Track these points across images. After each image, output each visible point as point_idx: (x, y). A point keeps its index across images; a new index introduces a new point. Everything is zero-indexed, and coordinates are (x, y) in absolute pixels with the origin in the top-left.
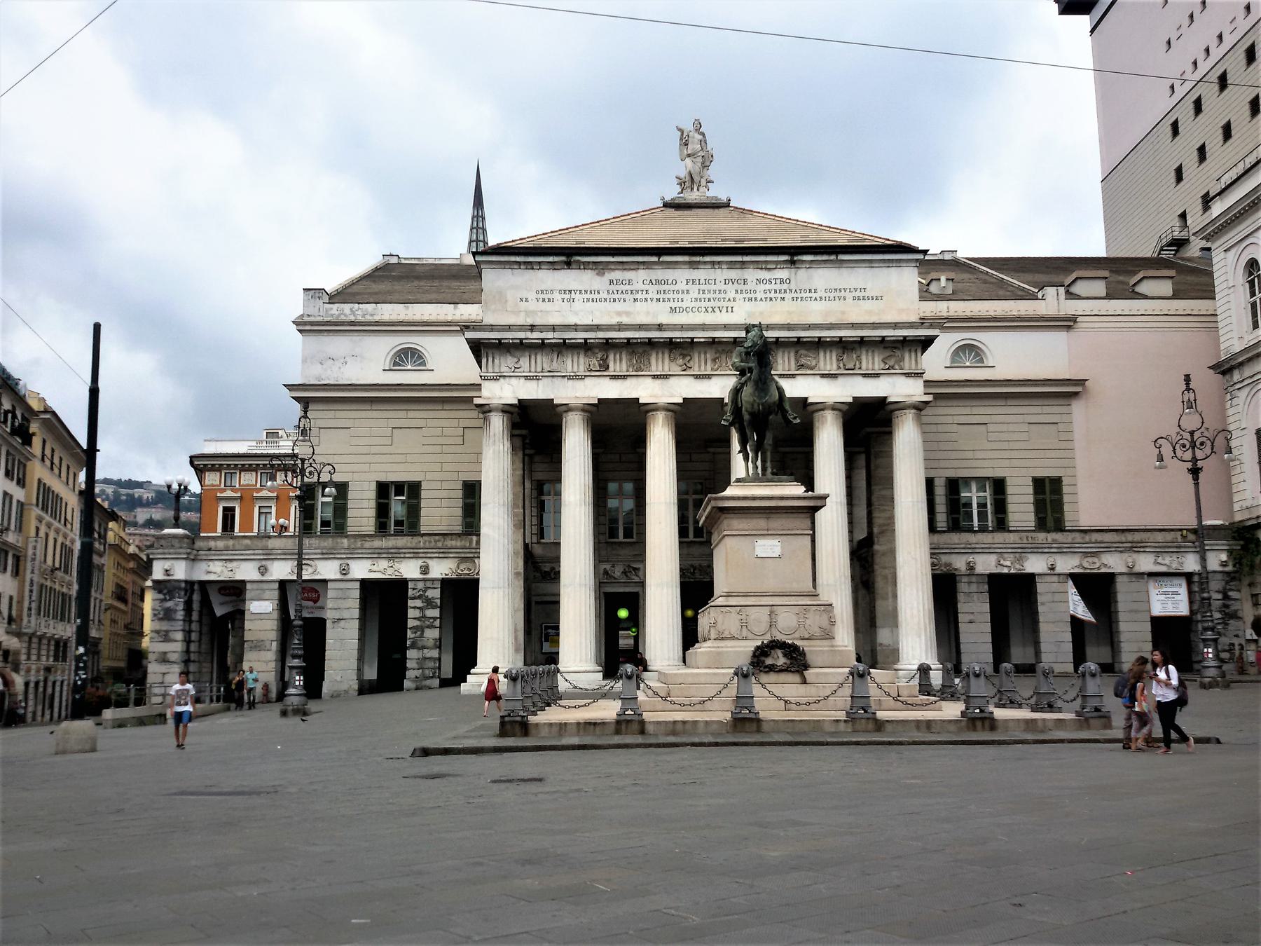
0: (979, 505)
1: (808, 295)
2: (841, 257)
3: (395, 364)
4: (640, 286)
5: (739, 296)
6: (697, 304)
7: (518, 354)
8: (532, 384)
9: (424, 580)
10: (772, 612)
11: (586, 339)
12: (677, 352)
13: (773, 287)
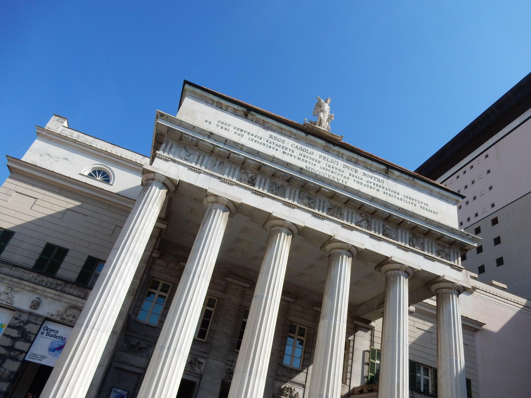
0: (424, 385)
1: (393, 194)
2: (415, 180)
3: (90, 175)
4: (289, 147)
5: (351, 177)
7: (190, 151)
8: (194, 175)
9: (30, 314)
13: (372, 180)
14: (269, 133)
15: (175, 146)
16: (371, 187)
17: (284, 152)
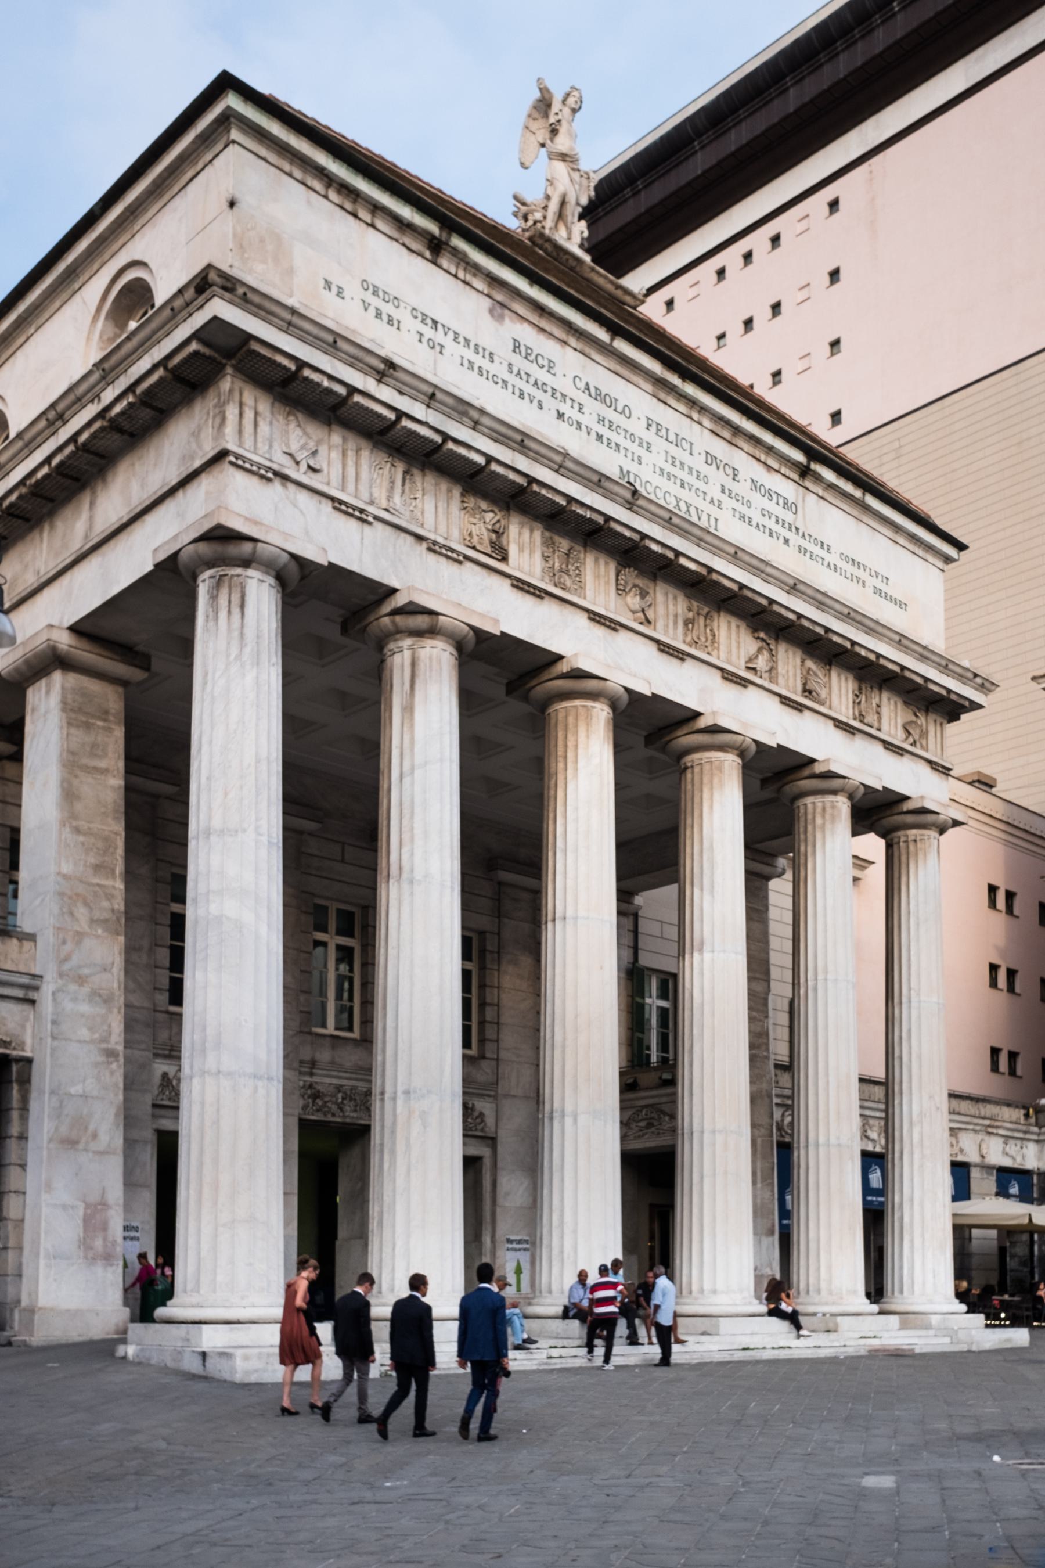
5: (724, 498)
11: (490, 459)
12: (630, 576)
15: (264, 406)
17: (560, 416)
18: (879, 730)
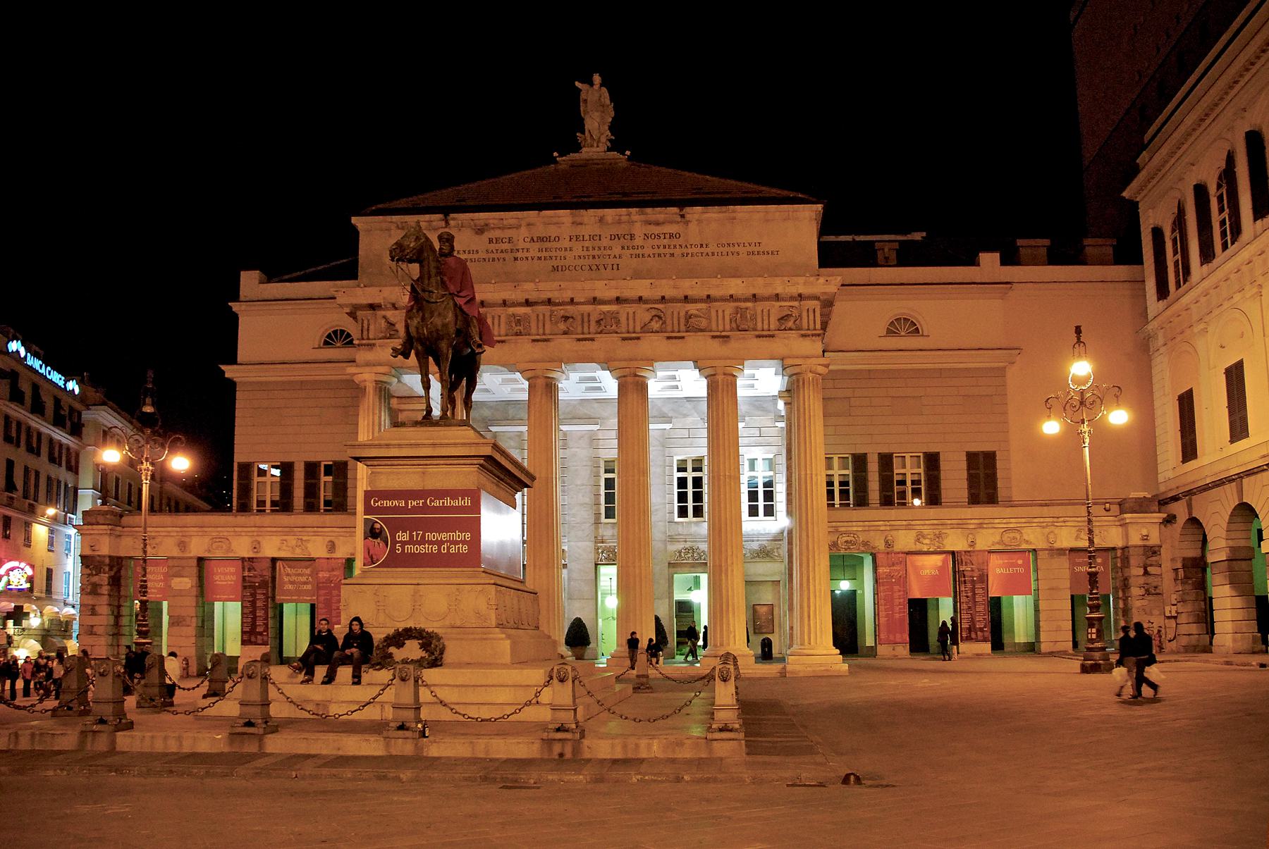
1: (699, 250)
4: (521, 245)
6: (581, 262)
10: (416, 592)
14: (487, 235)
16: (659, 255)
17: (516, 259)
18: (755, 330)
